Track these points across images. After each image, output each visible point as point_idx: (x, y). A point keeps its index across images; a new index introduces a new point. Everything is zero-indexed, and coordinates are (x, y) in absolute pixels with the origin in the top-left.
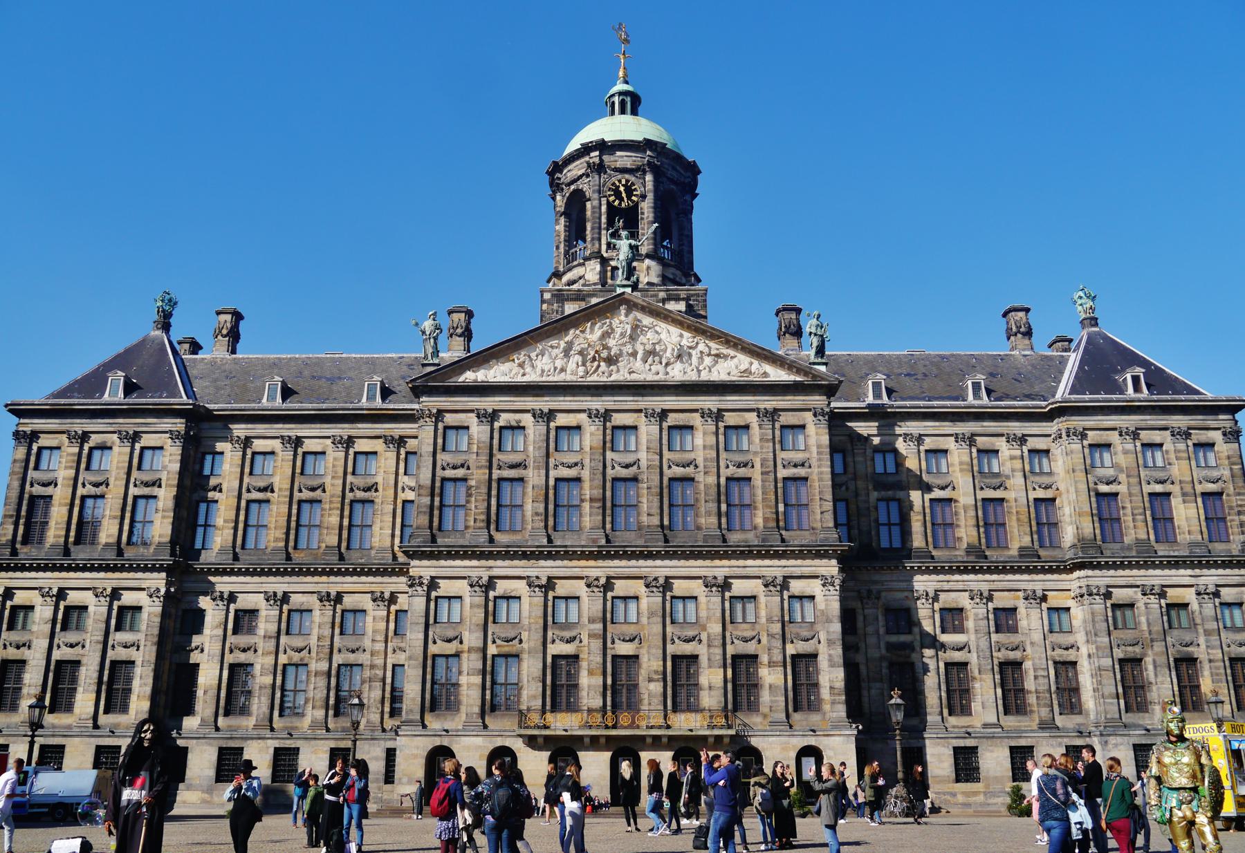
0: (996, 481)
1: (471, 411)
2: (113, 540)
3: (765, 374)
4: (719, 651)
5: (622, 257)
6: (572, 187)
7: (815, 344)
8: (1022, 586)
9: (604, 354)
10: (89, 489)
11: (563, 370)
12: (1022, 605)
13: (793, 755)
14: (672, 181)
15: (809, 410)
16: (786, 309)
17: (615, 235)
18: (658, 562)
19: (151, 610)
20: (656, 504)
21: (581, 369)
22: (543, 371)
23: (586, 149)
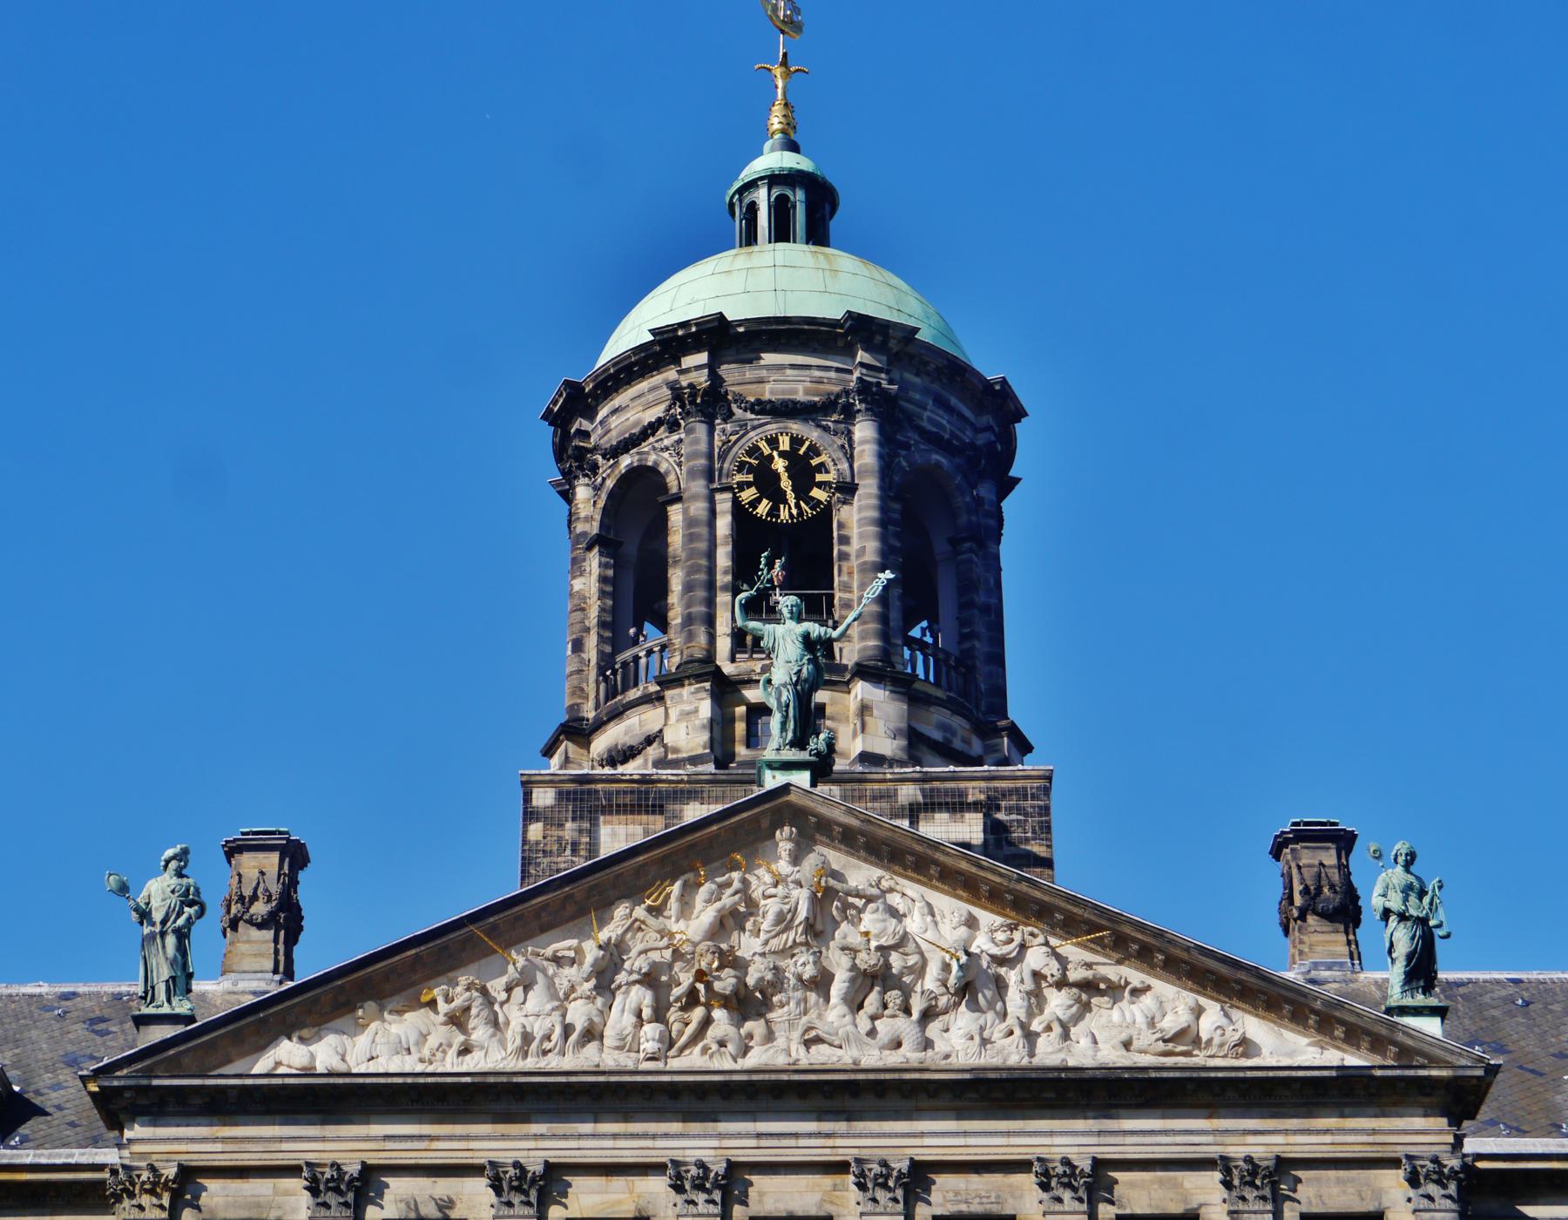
1: (292, 1171)
3: (1245, 1045)
5: (780, 675)
6: (626, 461)
7: (1403, 947)
9: (725, 983)
11: (592, 1034)
14: (935, 440)
15: (1394, 1163)
16: (1307, 835)
17: (760, 607)
21: (651, 1030)
22: (527, 1038)
23: (669, 345)
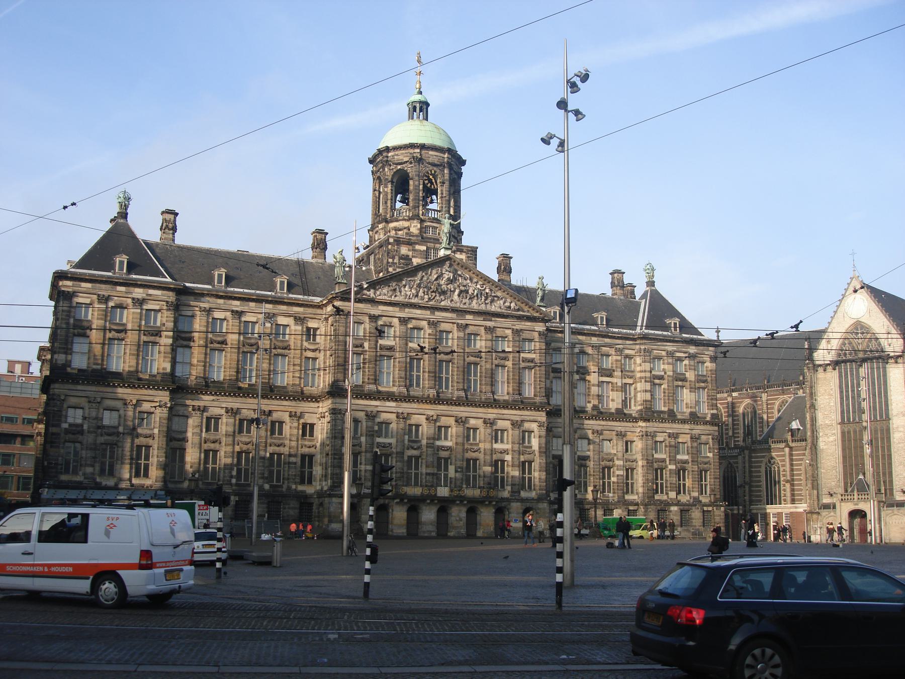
0: (607, 372)
2: (132, 369)
4: (488, 457)
6: (399, 167)
8: (616, 429)
10: (112, 334)
11: (417, 296)
12: (615, 438)
13: (521, 511)
18: (462, 408)
19: (160, 414)
20: (461, 377)
23: (412, 146)
